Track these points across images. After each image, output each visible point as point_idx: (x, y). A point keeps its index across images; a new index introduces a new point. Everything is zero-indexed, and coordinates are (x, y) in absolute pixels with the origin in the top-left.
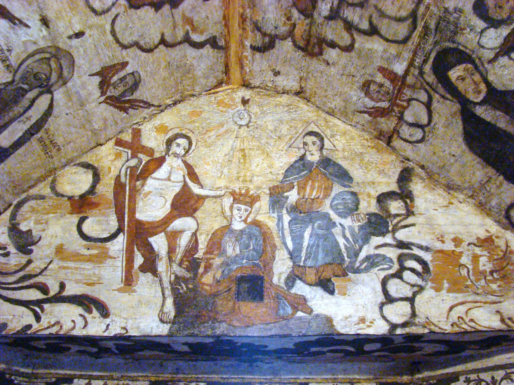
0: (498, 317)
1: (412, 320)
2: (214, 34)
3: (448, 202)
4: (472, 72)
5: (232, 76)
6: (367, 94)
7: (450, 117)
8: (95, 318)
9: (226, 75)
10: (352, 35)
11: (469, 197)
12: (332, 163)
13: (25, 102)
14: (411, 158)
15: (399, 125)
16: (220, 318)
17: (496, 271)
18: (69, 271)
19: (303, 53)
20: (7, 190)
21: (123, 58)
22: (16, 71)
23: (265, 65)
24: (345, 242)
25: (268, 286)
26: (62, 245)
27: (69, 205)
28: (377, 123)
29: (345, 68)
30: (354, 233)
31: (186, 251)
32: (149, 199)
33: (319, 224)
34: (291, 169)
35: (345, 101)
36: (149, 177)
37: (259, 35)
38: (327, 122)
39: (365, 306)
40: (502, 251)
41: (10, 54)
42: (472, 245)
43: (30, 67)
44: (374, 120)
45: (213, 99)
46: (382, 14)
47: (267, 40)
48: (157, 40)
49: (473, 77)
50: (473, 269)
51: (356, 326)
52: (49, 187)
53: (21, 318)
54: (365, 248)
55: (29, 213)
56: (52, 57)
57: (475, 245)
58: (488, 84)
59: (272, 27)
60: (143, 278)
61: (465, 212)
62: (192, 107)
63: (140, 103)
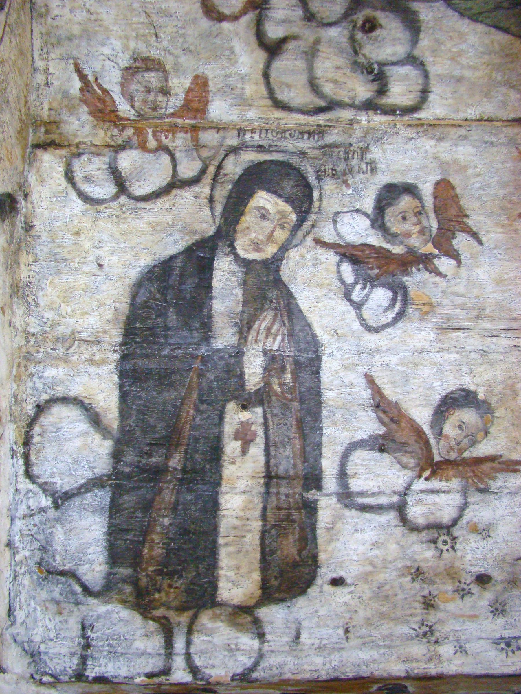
4: (286, 225)
6: (130, 72)
49: (278, 229)
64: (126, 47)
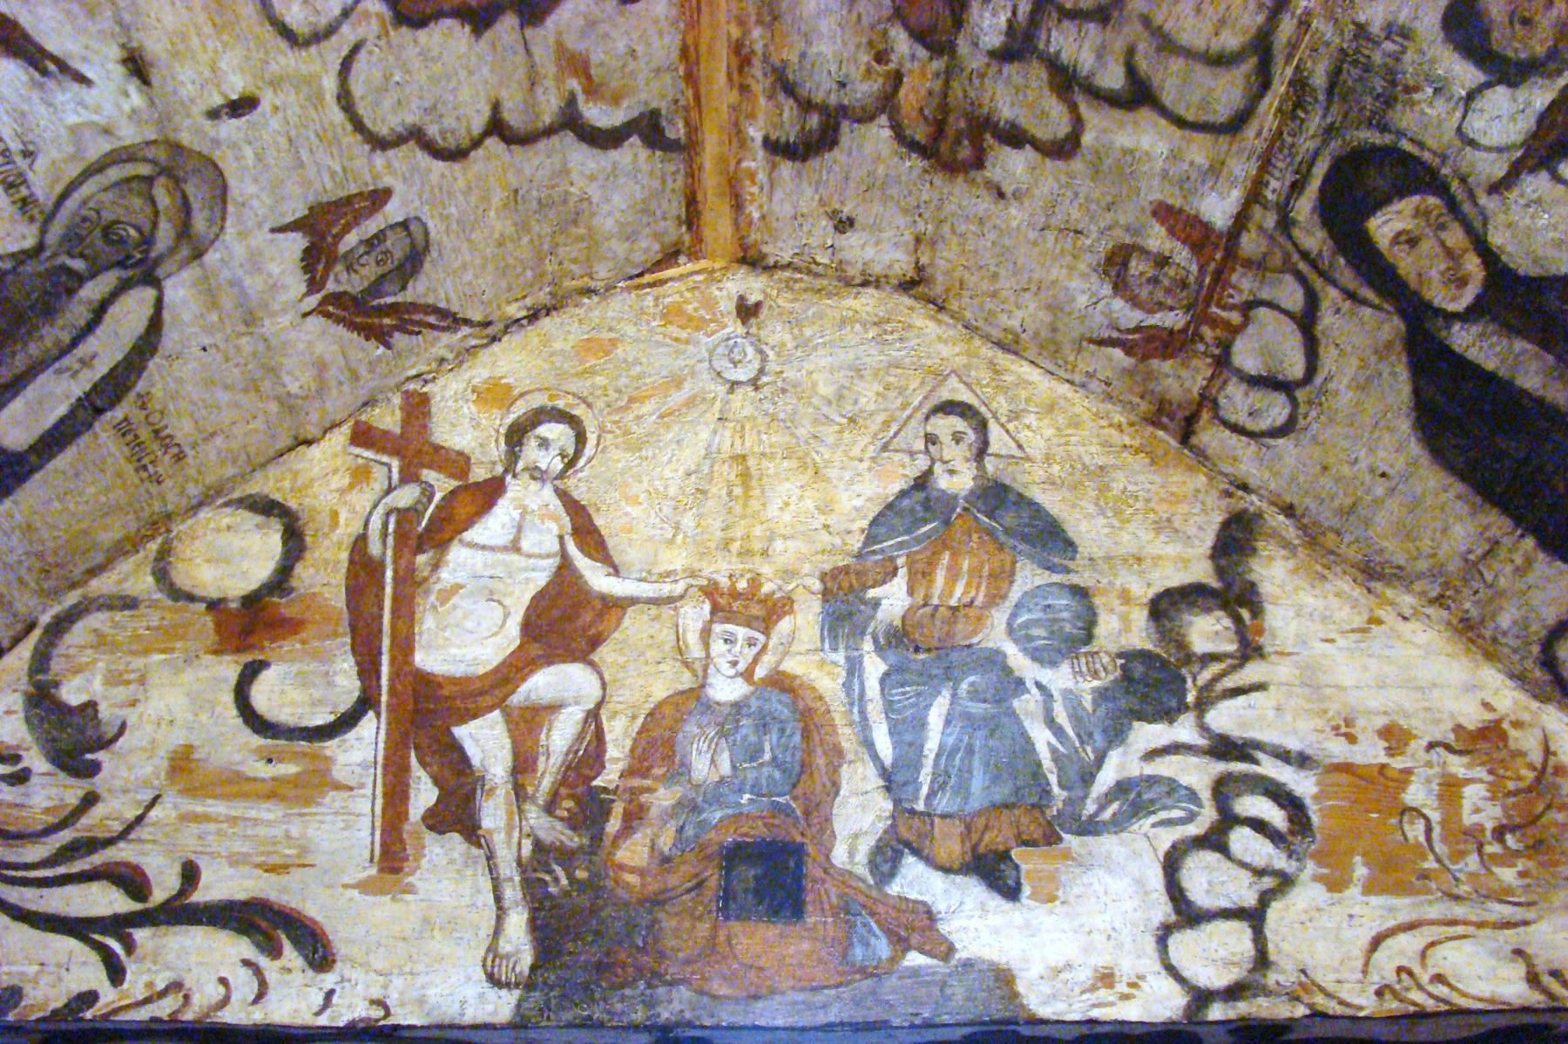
0: (1520, 969)
1: (1257, 976)
2: (654, 105)
3: (1366, 617)
4: (1442, 220)
5: (707, 233)
7: (1373, 359)
8: (289, 970)
9: (690, 228)
10: (1073, 108)
11: (1432, 602)
12: (1011, 497)
13: (76, 312)
14: (1253, 483)
15: (1217, 383)
16: (671, 970)
17: (1513, 829)
18: (212, 827)
19: (925, 164)
20: (21, 581)
21: (375, 178)
22: (49, 218)
23: (808, 199)
24: (1054, 741)
25: (819, 873)
26: (189, 748)
27: (211, 625)
28: (1150, 376)
29: (1051, 207)
30: (1080, 713)
31: (569, 768)
32: (455, 607)
33: (972, 684)
34: (888, 517)
35: (1054, 308)
36: (456, 542)
37: (789, 108)
38: (997, 372)
39: (1114, 934)
40: (1531, 767)
41: (31, 166)
42: (1440, 750)
43: (91, 204)
44: (1141, 367)
45: (649, 301)
46: (1166, 44)
47: (814, 121)
48: (478, 123)
49: (1443, 235)
50: (1443, 823)
51: (1085, 996)
52: (148, 570)
53: (63, 971)
54: (1114, 758)
55: (89, 651)
56: (159, 174)
57: (1449, 748)
58: (1488, 256)
59: (828, 84)
60: (438, 850)
61: (1419, 647)
62: (586, 328)
63: (427, 313)
64: (1085, 276)
